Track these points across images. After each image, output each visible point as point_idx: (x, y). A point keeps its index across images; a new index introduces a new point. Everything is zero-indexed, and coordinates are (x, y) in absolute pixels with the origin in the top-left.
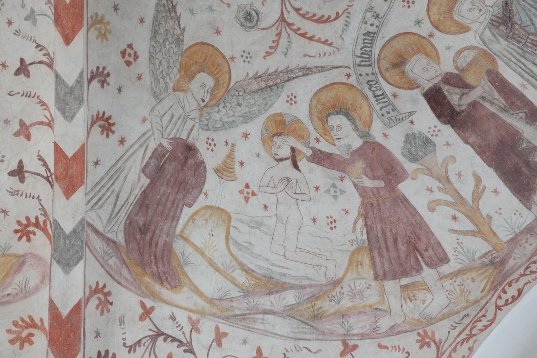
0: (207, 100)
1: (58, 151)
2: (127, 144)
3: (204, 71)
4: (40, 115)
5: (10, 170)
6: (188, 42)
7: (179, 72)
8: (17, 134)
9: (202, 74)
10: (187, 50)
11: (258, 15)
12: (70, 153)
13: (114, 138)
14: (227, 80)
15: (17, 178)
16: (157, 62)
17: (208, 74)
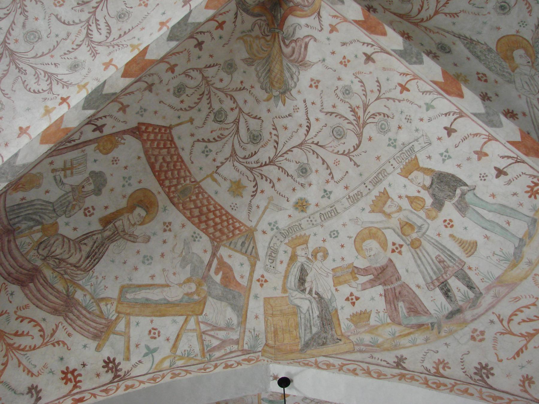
0: (530, 60)
1: (513, 143)
2: (527, 113)
3: (514, 50)
4: (480, 141)
5: (495, 176)
6: (493, 47)
7: (506, 62)
8: (479, 159)
9: (515, 52)
10: (497, 50)
11: (505, 2)
12: (518, 138)
13: (520, 116)
14: (527, 43)
15: (502, 175)
16: (493, 68)
17: (517, 49)
